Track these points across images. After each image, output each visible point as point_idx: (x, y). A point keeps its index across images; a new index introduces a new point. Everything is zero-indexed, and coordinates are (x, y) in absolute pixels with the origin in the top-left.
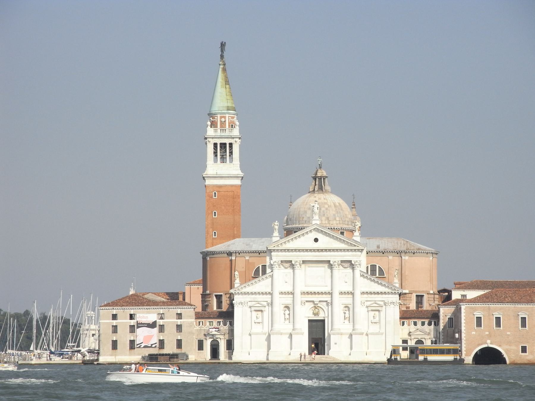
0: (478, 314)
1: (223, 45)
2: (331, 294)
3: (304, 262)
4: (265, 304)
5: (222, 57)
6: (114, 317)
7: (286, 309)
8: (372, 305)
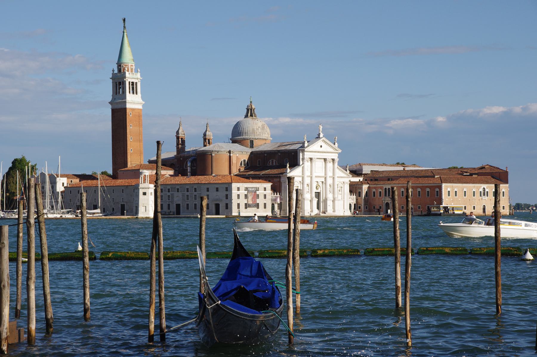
0: (449, 190)
3: (317, 158)
5: (124, 27)
6: (238, 189)
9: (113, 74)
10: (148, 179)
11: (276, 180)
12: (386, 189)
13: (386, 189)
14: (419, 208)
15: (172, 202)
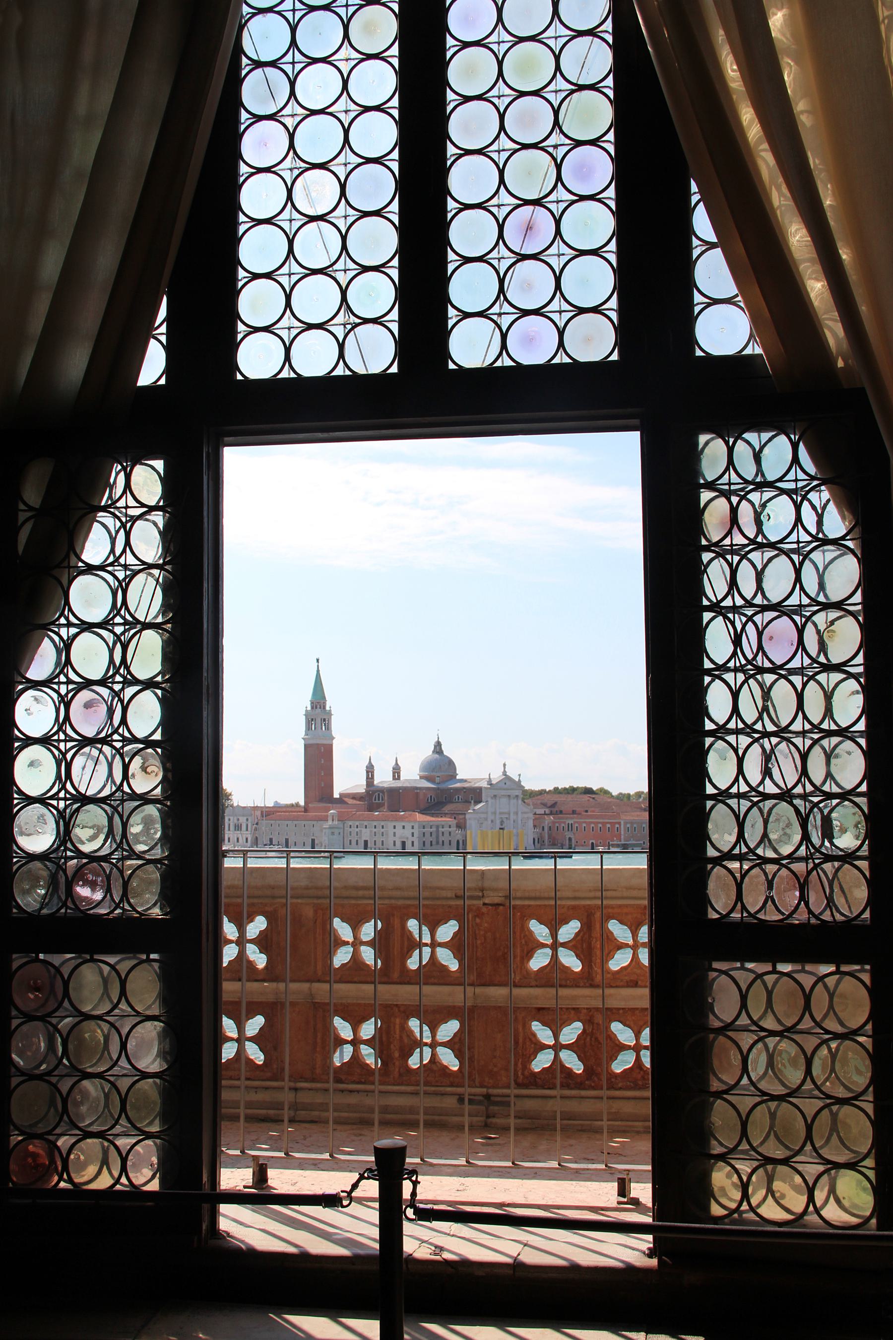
0: (628, 825)
5: (318, 666)
9: (306, 711)
10: (336, 818)
12: (568, 824)
13: (568, 824)
14: (600, 843)
15: (360, 838)
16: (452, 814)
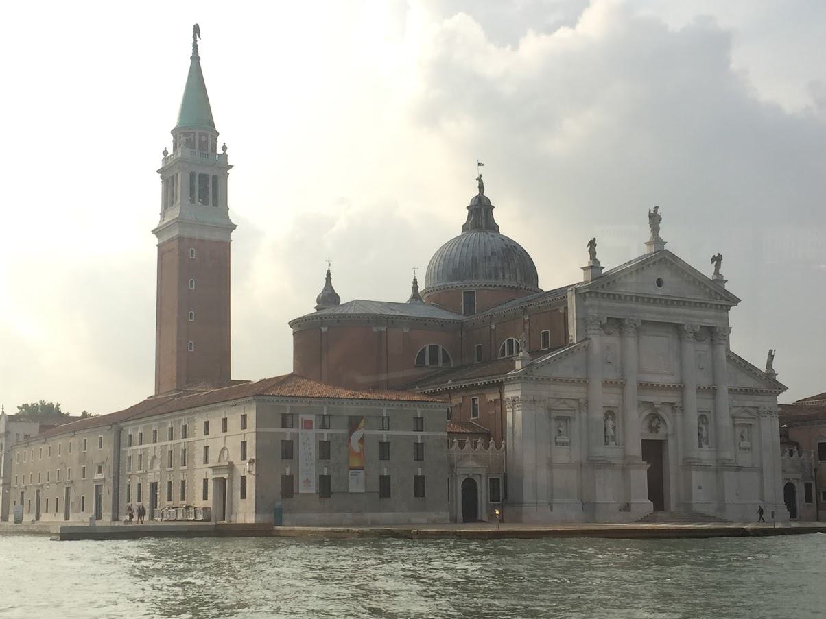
1: (196, 29)
2: (680, 389)
3: (644, 322)
4: (574, 404)
5: (195, 46)
7: (610, 416)
8: (742, 415)
9: (165, 160)
11: (492, 397)
16: (466, 389)
